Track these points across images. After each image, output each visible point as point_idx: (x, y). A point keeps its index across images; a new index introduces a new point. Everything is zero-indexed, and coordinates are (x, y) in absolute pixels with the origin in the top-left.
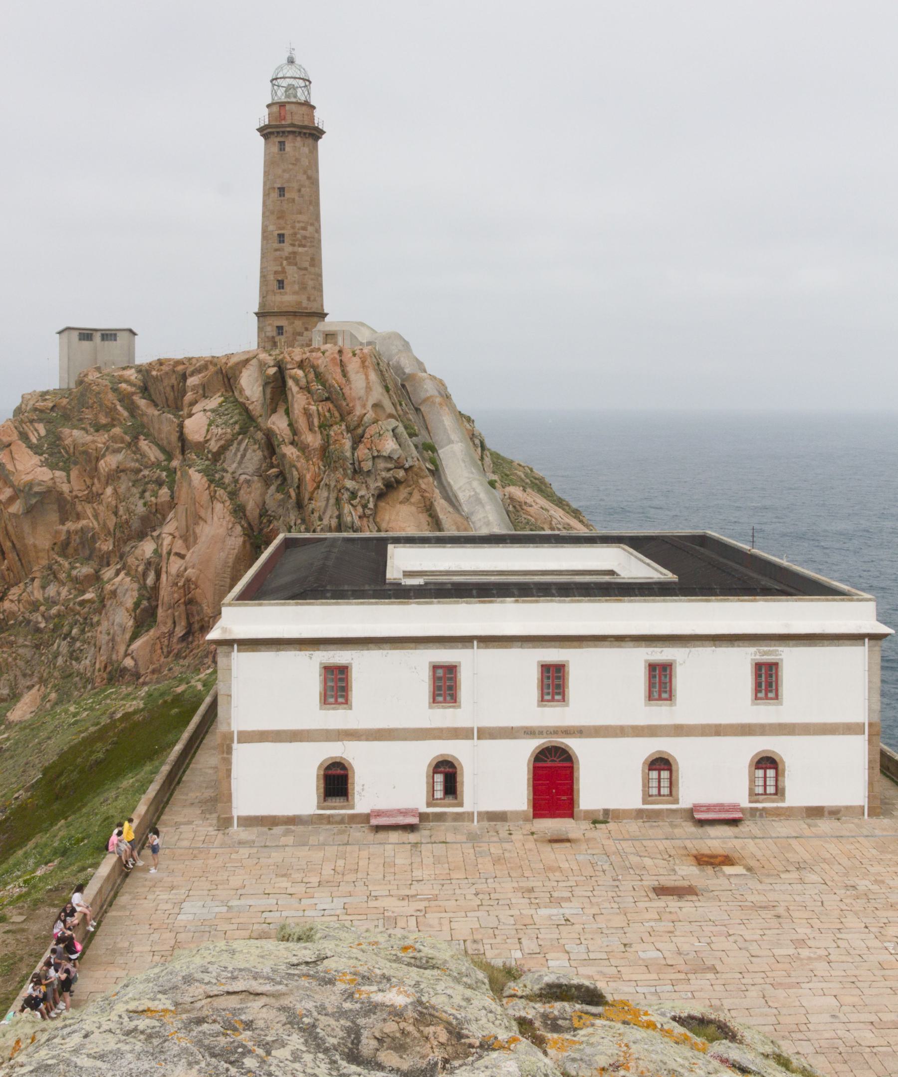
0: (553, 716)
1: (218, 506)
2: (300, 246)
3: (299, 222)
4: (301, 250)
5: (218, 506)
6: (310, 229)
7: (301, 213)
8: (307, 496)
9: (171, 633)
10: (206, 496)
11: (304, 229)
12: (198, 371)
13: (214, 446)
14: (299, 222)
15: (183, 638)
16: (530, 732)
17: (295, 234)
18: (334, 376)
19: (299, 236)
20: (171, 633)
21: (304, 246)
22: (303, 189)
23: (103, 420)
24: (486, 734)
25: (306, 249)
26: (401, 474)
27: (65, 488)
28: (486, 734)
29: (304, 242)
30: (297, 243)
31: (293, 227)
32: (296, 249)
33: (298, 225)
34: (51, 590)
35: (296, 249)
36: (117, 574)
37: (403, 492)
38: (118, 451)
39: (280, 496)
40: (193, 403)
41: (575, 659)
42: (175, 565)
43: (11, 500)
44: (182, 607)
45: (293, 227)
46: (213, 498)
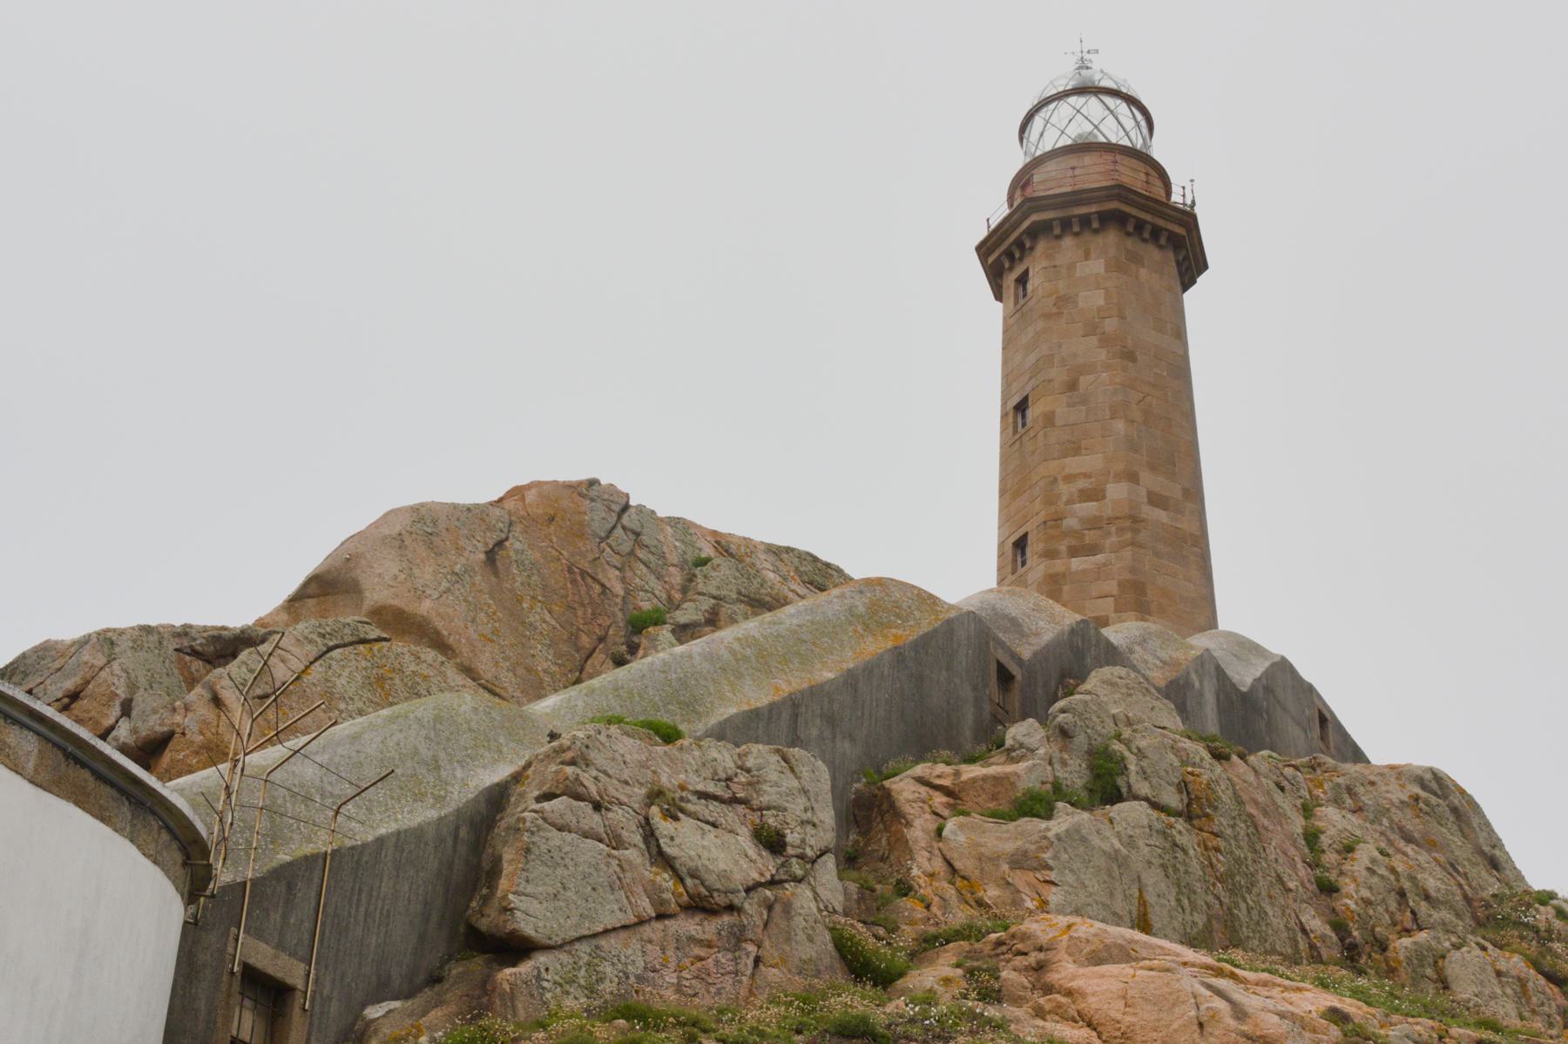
2: (1074, 552)
3: (1069, 478)
4: (1077, 564)
6: (1117, 492)
7: (1077, 451)
11: (1095, 494)
14: (1069, 478)
17: (1057, 519)
19: (1071, 522)
21: (1092, 550)
22: (1084, 381)
25: (1100, 558)
29: (1090, 537)
30: (1063, 548)
31: (1050, 500)
32: (1058, 566)
33: (1064, 489)
35: (1058, 566)
45: (1050, 500)
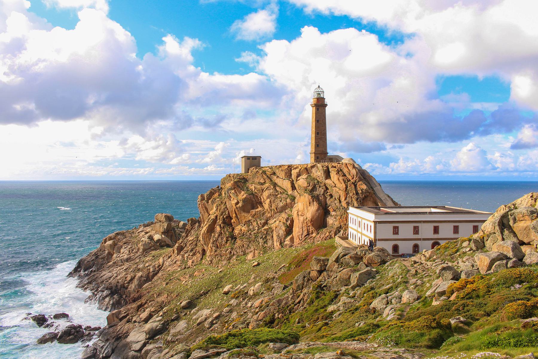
0: (436, 236)
1: (315, 202)
5: (315, 202)
8: (343, 199)
9: (302, 235)
10: (311, 200)
12: (296, 168)
13: (310, 188)
15: (306, 236)
16: (432, 239)
18: (345, 170)
20: (302, 235)
23: (262, 181)
24: (424, 239)
26: (368, 194)
27: (254, 200)
28: (424, 239)
34: (251, 227)
36: (275, 221)
37: (369, 198)
38: (270, 190)
39: (331, 200)
40: (298, 177)
41: (440, 225)
42: (301, 219)
43: (237, 203)
44: (306, 228)
46: (313, 201)
